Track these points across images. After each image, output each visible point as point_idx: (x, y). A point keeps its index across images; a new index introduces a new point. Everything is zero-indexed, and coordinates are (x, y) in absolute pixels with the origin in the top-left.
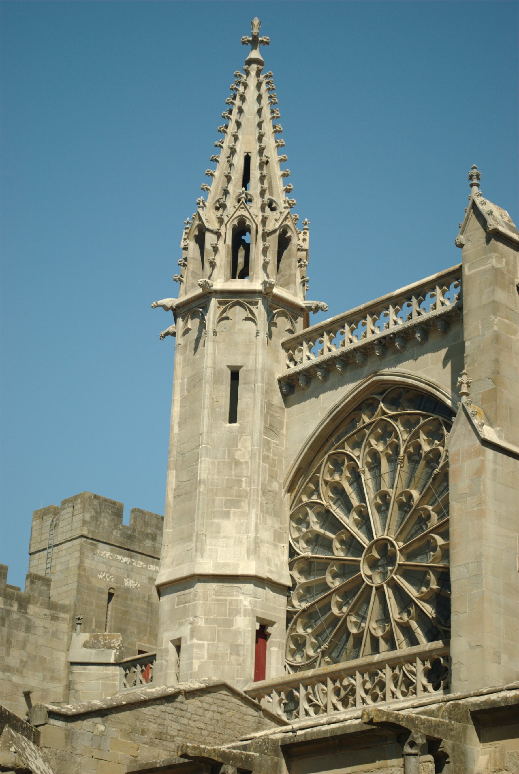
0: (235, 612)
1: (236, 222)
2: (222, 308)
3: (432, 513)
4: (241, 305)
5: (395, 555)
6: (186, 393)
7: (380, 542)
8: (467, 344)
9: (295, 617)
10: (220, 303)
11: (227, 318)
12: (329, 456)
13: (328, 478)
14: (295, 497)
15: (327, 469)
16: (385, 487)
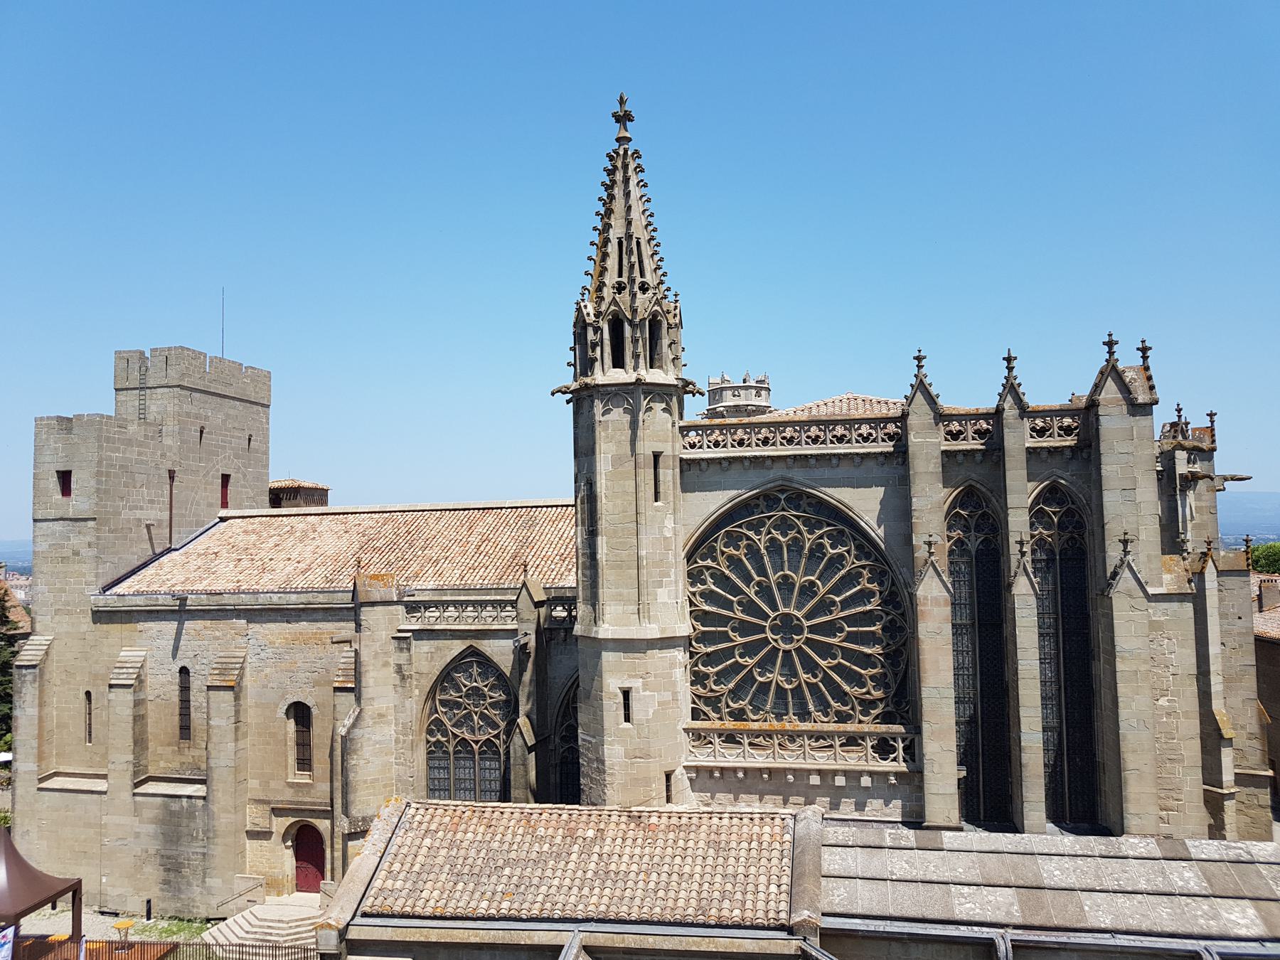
0: (672, 665)
13: (724, 549)
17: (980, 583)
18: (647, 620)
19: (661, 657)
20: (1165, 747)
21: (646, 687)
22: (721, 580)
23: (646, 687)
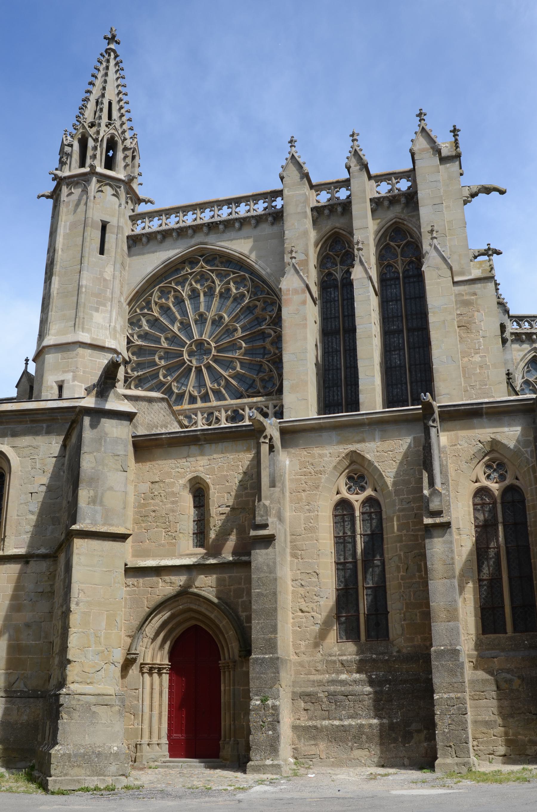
1: (109, 136)
2: (99, 185)
3: (239, 328)
4: (110, 186)
5: (211, 350)
6: (68, 231)
7: (199, 341)
8: (286, 232)
9: (130, 380)
10: (98, 181)
11: (102, 191)
12: (160, 287)
14: (132, 309)
15: (157, 295)
16: (202, 309)
17: (345, 302)
18: (80, 330)
19: (90, 360)
20: (479, 391)
21: (74, 378)
22: (154, 323)
23: (74, 378)
